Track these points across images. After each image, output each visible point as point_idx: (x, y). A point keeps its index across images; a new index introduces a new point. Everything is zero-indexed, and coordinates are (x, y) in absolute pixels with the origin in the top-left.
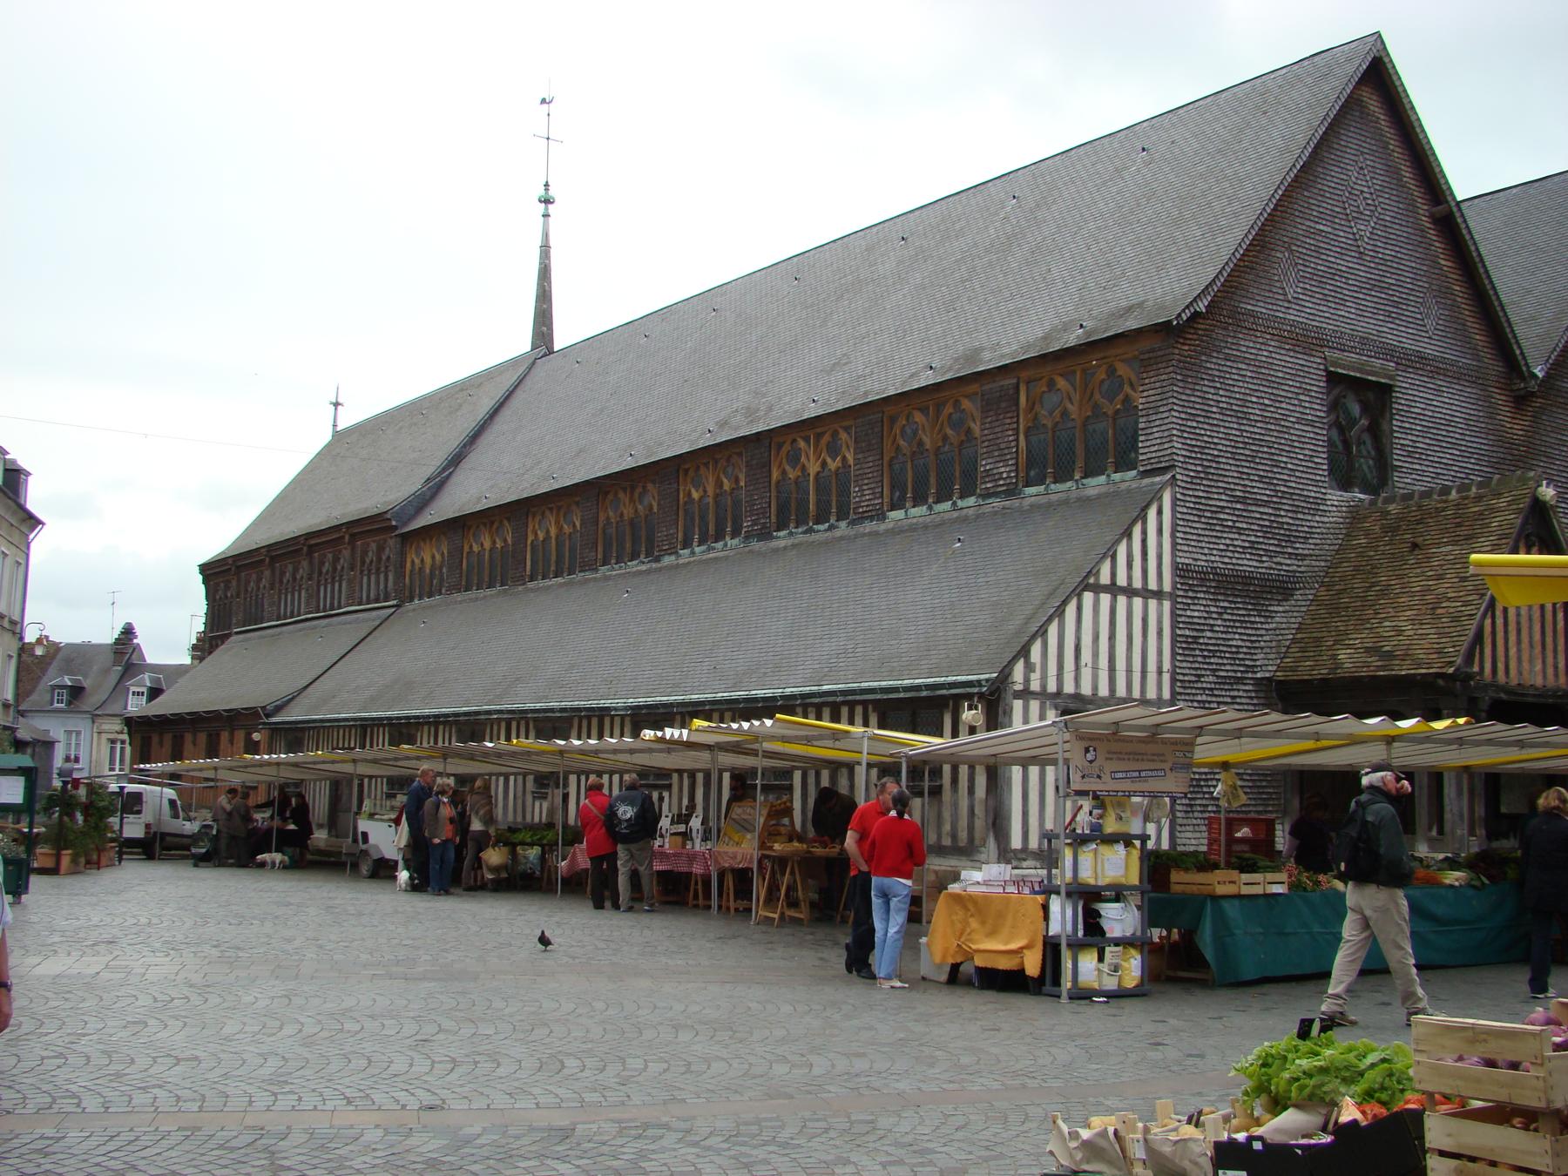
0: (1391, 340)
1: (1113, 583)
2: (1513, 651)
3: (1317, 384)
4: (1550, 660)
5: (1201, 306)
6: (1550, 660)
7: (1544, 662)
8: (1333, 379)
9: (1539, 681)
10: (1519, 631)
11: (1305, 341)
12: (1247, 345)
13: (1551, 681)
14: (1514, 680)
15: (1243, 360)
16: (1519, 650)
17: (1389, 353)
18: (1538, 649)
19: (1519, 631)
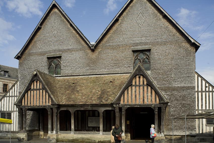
0: (61, 48)
1: (9, 96)
2: (32, 100)
3: (45, 59)
4: (41, 100)
5: (19, 55)
6: (41, 100)
7: (39, 101)
8: (48, 58)
9: (38, 105)
10: (34, 97)
11: (42, 54)
12: (32, 58)
13: (41, 104)
14: (32, 105)
15: (30, 60)
16: (34, 100)
17: (60, 51)
18: (38, 99)
19: (34, 97)
